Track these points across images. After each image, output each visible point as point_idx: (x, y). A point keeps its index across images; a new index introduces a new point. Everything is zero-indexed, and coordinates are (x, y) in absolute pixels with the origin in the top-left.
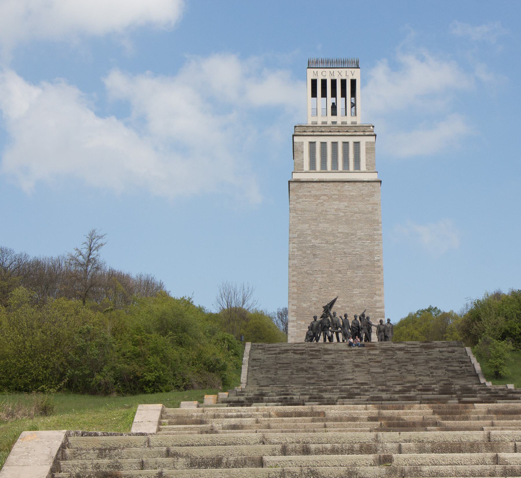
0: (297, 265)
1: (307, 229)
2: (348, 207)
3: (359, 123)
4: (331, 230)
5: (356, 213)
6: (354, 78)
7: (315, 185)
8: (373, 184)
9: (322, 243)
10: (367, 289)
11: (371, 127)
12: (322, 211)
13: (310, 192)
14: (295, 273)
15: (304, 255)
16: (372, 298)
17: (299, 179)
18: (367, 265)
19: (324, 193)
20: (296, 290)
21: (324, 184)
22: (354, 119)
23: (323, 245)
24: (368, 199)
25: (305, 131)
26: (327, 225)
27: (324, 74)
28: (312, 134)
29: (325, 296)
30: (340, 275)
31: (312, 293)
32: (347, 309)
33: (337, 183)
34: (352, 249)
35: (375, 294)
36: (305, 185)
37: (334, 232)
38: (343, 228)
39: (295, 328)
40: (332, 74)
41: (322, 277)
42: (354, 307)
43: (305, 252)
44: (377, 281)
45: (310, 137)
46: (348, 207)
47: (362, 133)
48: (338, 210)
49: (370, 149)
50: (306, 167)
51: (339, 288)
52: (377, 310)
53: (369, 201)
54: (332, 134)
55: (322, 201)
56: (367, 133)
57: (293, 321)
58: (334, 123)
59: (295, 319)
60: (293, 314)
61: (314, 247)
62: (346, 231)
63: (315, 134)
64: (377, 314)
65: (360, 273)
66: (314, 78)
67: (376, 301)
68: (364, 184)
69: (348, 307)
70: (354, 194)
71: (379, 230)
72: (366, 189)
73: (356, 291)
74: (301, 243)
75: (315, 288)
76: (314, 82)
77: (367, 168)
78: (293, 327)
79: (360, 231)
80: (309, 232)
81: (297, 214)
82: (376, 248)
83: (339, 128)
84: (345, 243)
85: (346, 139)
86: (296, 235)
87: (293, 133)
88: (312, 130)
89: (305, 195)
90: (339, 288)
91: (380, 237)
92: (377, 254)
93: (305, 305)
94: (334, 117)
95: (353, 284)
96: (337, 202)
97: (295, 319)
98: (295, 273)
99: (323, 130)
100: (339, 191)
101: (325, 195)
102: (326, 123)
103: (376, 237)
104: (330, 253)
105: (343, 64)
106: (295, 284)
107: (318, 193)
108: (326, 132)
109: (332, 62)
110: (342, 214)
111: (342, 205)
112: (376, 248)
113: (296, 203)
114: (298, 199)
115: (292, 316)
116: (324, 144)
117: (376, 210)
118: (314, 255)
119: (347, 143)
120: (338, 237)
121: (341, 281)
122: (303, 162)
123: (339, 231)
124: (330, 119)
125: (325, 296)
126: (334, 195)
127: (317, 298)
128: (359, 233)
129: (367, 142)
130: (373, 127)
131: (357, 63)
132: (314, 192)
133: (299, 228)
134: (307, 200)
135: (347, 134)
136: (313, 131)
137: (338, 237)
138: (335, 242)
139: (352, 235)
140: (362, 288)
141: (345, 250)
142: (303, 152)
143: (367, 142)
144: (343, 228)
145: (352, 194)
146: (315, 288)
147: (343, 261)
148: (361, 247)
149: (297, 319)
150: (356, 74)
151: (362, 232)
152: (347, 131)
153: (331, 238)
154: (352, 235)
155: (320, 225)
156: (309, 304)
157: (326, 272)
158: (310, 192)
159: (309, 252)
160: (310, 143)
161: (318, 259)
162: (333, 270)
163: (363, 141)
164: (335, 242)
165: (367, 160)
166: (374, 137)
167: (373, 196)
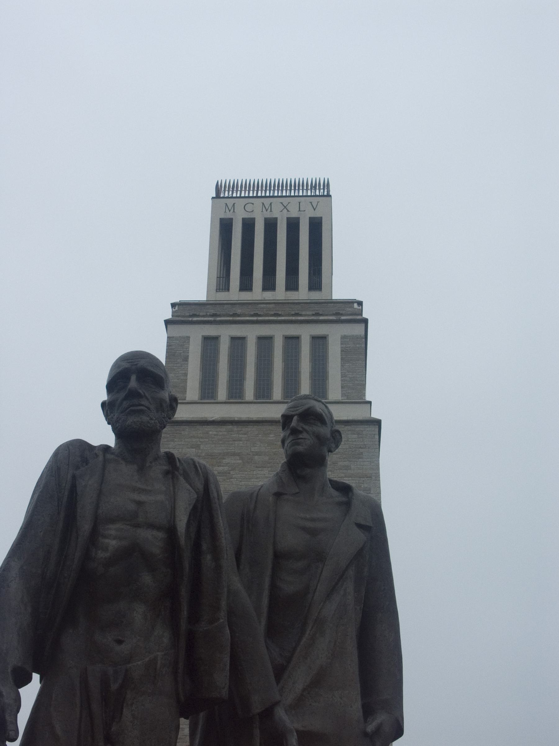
6: (318, 215)
7: (212, 431)
11: (356, 305)
13: (197, 447)
21: (235, 428)
24: (346, 463)
27: (249, 208)
45: (207, 327)
53: (347, 468)
55: (226, 468)
66: (229, 215)
85: (292, 330)
87: (169, 316)
88: (212, 311)
99: (239, 311)
101: (234, 454)
108: (245, 315)
119: (297, 338)
122: (185, 381)
126: (257, 454)
129: (344, 337)
130: (360, 303)
131: (327, 186)
142: (186, 359)
143: (344, 337)
158: (197, 447)
160: (206, 339)
163: (335, 334)
166: (363, 326)
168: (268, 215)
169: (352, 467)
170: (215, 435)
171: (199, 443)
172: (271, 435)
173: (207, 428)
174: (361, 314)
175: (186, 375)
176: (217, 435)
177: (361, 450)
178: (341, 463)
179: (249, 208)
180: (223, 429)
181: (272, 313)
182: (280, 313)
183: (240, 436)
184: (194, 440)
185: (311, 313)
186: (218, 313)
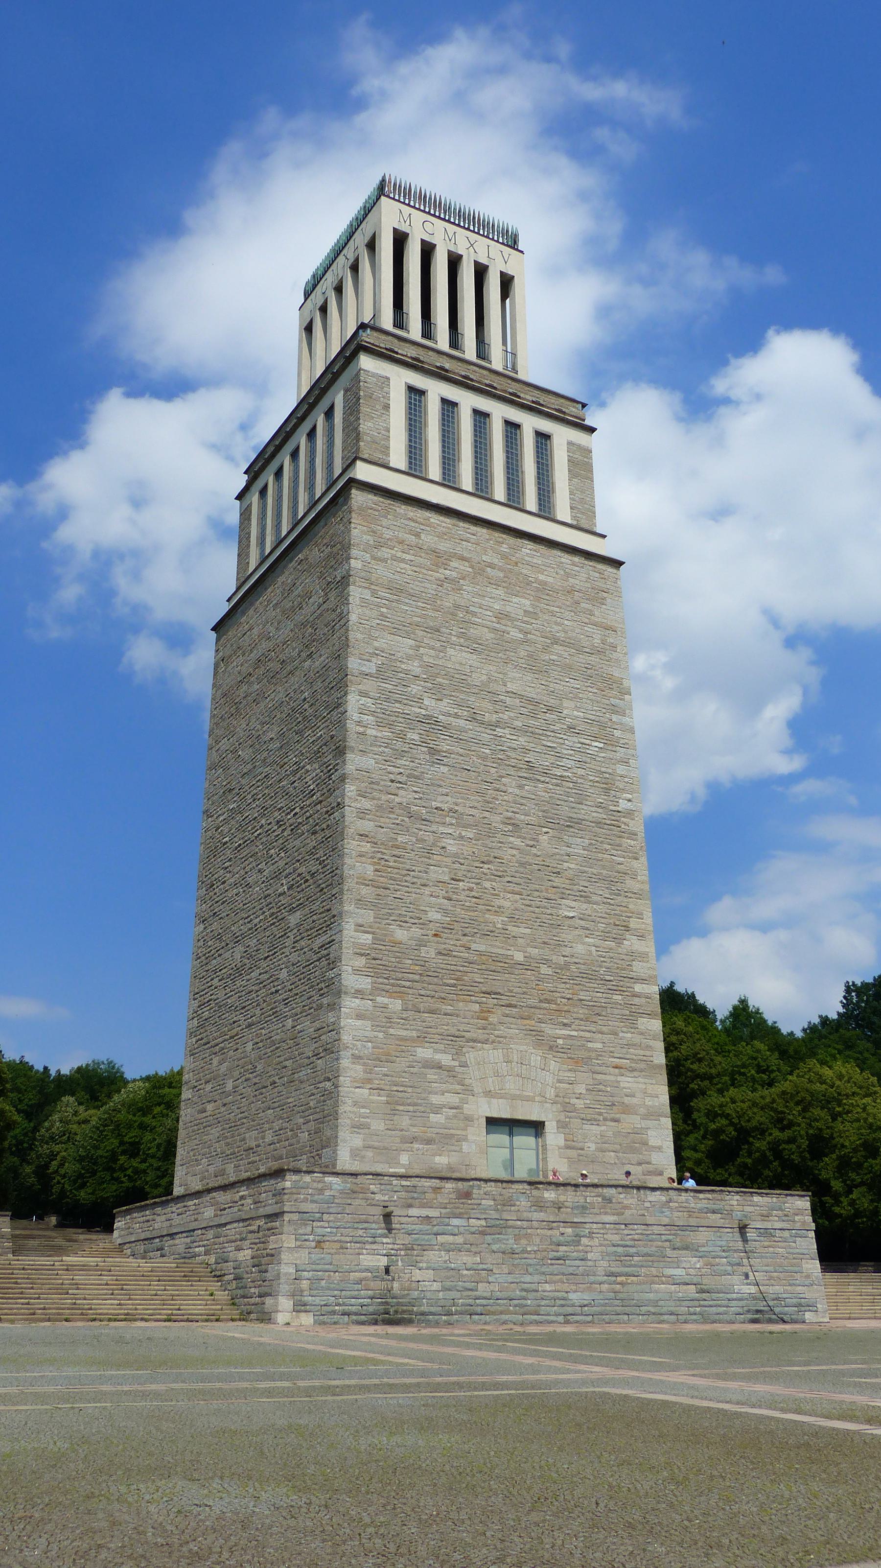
0: (375, 776)
1: (409, 657)
2: (534, 615)
4: (484, 678)
5: (556, 641)
6: (510, 273)
7: (435, 518)
8: (600, 566)
9: (456, 716)
10: (602, 908)
12: (457, 607)
13: (417, 535)
14: (366, 804)
15: (399, 745)
16: (619, 940)
18: (598, 823)
19: (459, 550)
20: (370, 870)
23: (462, 723)
24: (589, 607)
26: (473, 659)
29: (469, 909)
30: (517, 842)
31: (427, 891)
32: (544, 969)
34: (552, 759)
35: (627, 928)
36: (402, 509)
37: (493, 687)
38: (519, 681)
39: (368, 1023)
40: (453, 238)
41: (461, 837)
42: (567, 964)
43: (401, 736)
44: (630, 884)
48: (501, 616)
49: (582, 466)
50: (398, 457)
51: (517, 889)
52: (638, 988)
55: (454, 574)
57: (359, 993)
59: (365, 983)
60: (361, 962)
61: (429, 722)
62: (531, 693)
64: (636, 1001)
65: (578, 844)
67: (633, 955)
68: (576, 559)
69: (547, 962)
70: (550, 580)
71: (624, 715)
73: (569, 908)
74: (387, 700)
76: (400, 240)
78: (359, 1017)
79: (571, 704)
80: (415, 667)
81: (374, 593)
82: (621, 769)
83: (493, 377)
84: (525, 730)
86: (371, 667)
89: (401, 542)
91: (628, 735)
92: (623, 790)
93: (401, 934)
95: (557, 882)
96: (500, 592)
97: (365, 983)
98: (366, 804)
99: (447, 366)
100: (504, 556)
101: (463, 559)
103: (617, 733)
104: (485, 758)
106: (367, 847)
107: (444, 546)
108: (454, 373)
109: (448, 209)
111: (520, 604)
112: (621, 769)
113: (374, 558)
114: (378, 546)
115: (357, 971)
117: (614, 647)
118: (433, 751)
121: (522, 864)
123: (510, 687)
125: (469, 909)
126: (491, 566)
127: (446, 912)
128: (569, 708)
129: (570, 443)
132: (428, 539)
134: (404, 556)
138: (497, 724)
139: (550, 709)
140: (586, 898)
141: (530, 757)
142: (387, 407)
143: (570, 443)
144: (519, 681)
145: (541, 577)
147: (524, 794)
148: (578, 757)
149: (376, 990)
151: (577, 708)
154: (550, 709)
155: (451, 651)
156: (416, 931)
158: (417, 535)
159: (416, 737)
161: (445, 769)
164: (497, 724)
165: (571, 493)
169: (596, 613)
170: (438, 525)
171: (418, 530)
172: (504, 546)
173: (427, 514)
174: (584, 420)
175: (389, 432)
176: (440, 526)
177: (605, 595)
178: (583, 605)
181: (487, 382)
182: (495, 385)
183: (469, 535)
184: (413, 524)
185: (531, 398)
186: (422, 358)
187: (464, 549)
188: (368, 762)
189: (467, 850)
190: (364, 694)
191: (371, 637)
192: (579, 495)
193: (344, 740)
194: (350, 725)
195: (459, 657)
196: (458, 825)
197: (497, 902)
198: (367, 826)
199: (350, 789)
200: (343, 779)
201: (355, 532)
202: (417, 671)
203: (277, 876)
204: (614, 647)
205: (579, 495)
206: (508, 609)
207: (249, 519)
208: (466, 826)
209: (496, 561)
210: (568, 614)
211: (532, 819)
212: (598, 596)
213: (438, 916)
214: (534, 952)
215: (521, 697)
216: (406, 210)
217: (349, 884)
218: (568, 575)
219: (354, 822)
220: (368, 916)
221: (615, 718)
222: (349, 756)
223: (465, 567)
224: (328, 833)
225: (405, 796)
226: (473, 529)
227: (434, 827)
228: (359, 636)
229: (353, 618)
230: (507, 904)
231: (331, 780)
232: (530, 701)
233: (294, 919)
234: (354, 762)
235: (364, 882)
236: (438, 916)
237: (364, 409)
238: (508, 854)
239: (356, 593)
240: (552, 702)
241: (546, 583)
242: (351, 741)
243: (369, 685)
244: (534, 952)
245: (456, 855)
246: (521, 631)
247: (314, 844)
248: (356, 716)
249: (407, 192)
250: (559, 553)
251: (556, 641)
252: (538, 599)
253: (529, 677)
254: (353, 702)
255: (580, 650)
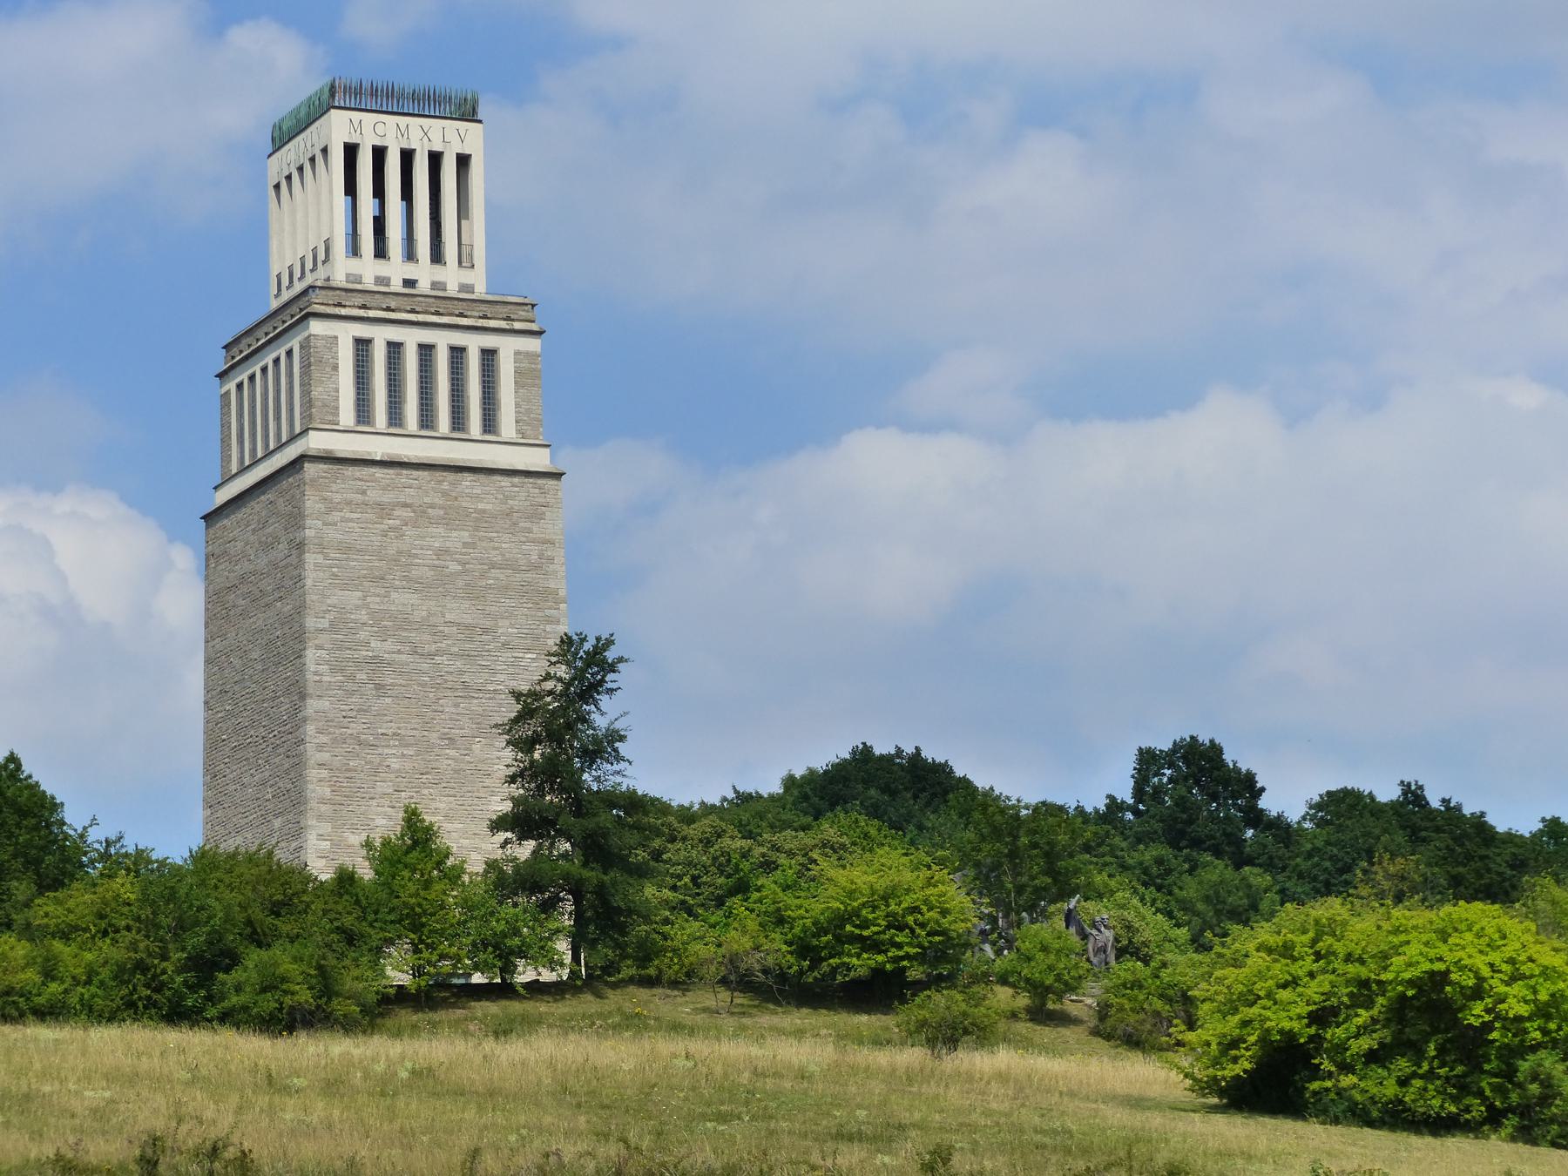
0: (331, 716)
1: (357, 608)
2: (473, 545)
3: (480, 290)
5: (493, 566)
7: (379, 472)
8: (540, 481)
9: (399, 652)
12: (400, 553)
13: (364, 493)
14: (324, 739)
15: (350, 686)
17: (331, 451)
19: (402, 499)
20: (327, 792)
22: (467, 277)
23: (403, 657)
24: (528, 525)
25: (339, 305)
26: (413, 599)
27: (380, 129)
28: (362, 313)
30: (452, 753)
31: (374, 802)
33: (438, 474)
34: (486, 676)
36: (350, 471)
37: (433, 620)
38: (457, 611)
41: (403, 755)
43: (352, 678)
46: (473, 545)
47: (503, 324)
48: (442, 552)
50: (347, 416)
51: (452, 792)
54: (421, 318)
56: (518, 326)
58: (410, 283)
61: (376, 662)
62: (468, 620)
63: (372, 314)
68: (516, 480)
70: (489, 507)
72: (521, 493)
75: (381, 788)
76: (351, 151)
77: (518, 431)
79: (507, 623)
80: (363, 616)
84: (465, 655)
85: (459, 339)
86: (325, 623)
89: (349, 503)
90: (452, 792)
94: (354, 261)
95: (488, 782)
96: (441, 530)
98: (324, 739)
99: (393, 305)
100: (445, 494)
101: (406, 505)
102: (381, 280)
104: (423, 685)
105: (427, 103)
106: (325, 773)
107: (387, 498)
109: (402, 96)
110: (454, 567)
113: (325, 524)
114: (329, 511)
116: (395, 348)
117: (551, 560)
118: (379, 687)
119: (462, 350)
120: (446, 637)
121: (456, 771)
123: (449, 617)
124: (396, 269)
126: (432, 506)
128: (505, 629)
129: (517, 353)
132: (373, 495)
133: (332, 601)
135: (338, 311)
136: (364, 307)
137: (446, 637)
139: (485, 631)
141: (466, 678)
142: (335, 368)
143: (517, 353)
144: (457, 611)
145: (481, 506)
146: (381, 788)
147: (460, 710)
148: (511, 670)
150: (448, 136)
151: (512, 625)
152: (461, 315)
153: (427, 637)
154: (485, 631)
155: (394, 595)
157: (412, 740)
158: (364, 493)
162: (434, 737)
163: (508, 348)
165: (517, 405)
167: (541, 517)
168: (405, 146)
169: (535, 529)
173: (373, 470)
179: (380, 129)
180: (391, 472)
187: (408, 495)
188: (324, 704)
189: (408, 766)
190: (319, 647)
191: (324, 596)
192: (525, 406)
193: (304, 687)
194: (309, 676)
195: (403, 599)
196: (401, 745)
197: (434, 805)
198: (325, 756)
199: (310, 729)
200: (305, 720)
201: (308, 504)
202: (365, 618)
203: (264, 783)
204: (551, 560)
205: (525, 406)
206: (448, 544)
207: (229, 445)
208: (407, 746)
209: (437, 500)
210: (506, 537)
211: (466, 731)
212: (536, 515)
213: (384, 822)
214: (465, 842)
215: (459, 624)
216: (356, 115)
217: (313, 804)
218: (507, 498)
219: (313, 756)
220: (326, 828)
221: (548, 628)
222: (309, 701)
223: (407, 513)
224: (296, 760)
225: (355, 728)
226: (415, 473)
227: (380, 750)
228: (315, 598)
229: (309, 582)
230: (442, 806)
231: (296, 720)
232: (467, 627)
233: (277, 823)
234: (312, 706)
235: (322, 801)
236: (384, 822)
237: (315, 375)
238: (444, 764)
239: (311, 558)
240: (488, 623)
241: (484, 511)
242: (310, 691)
243: (324, 639)
244: (465, 842)
245: (399, 771)
246: (459, 562)
247: (287, 766)
248: (313, 668)
249: (357, 92)
250: (499, 478)
251: (493, 566)
252: (477, 529)
253: (466, 604)
254: (311, 655)
255: (517, 570)
